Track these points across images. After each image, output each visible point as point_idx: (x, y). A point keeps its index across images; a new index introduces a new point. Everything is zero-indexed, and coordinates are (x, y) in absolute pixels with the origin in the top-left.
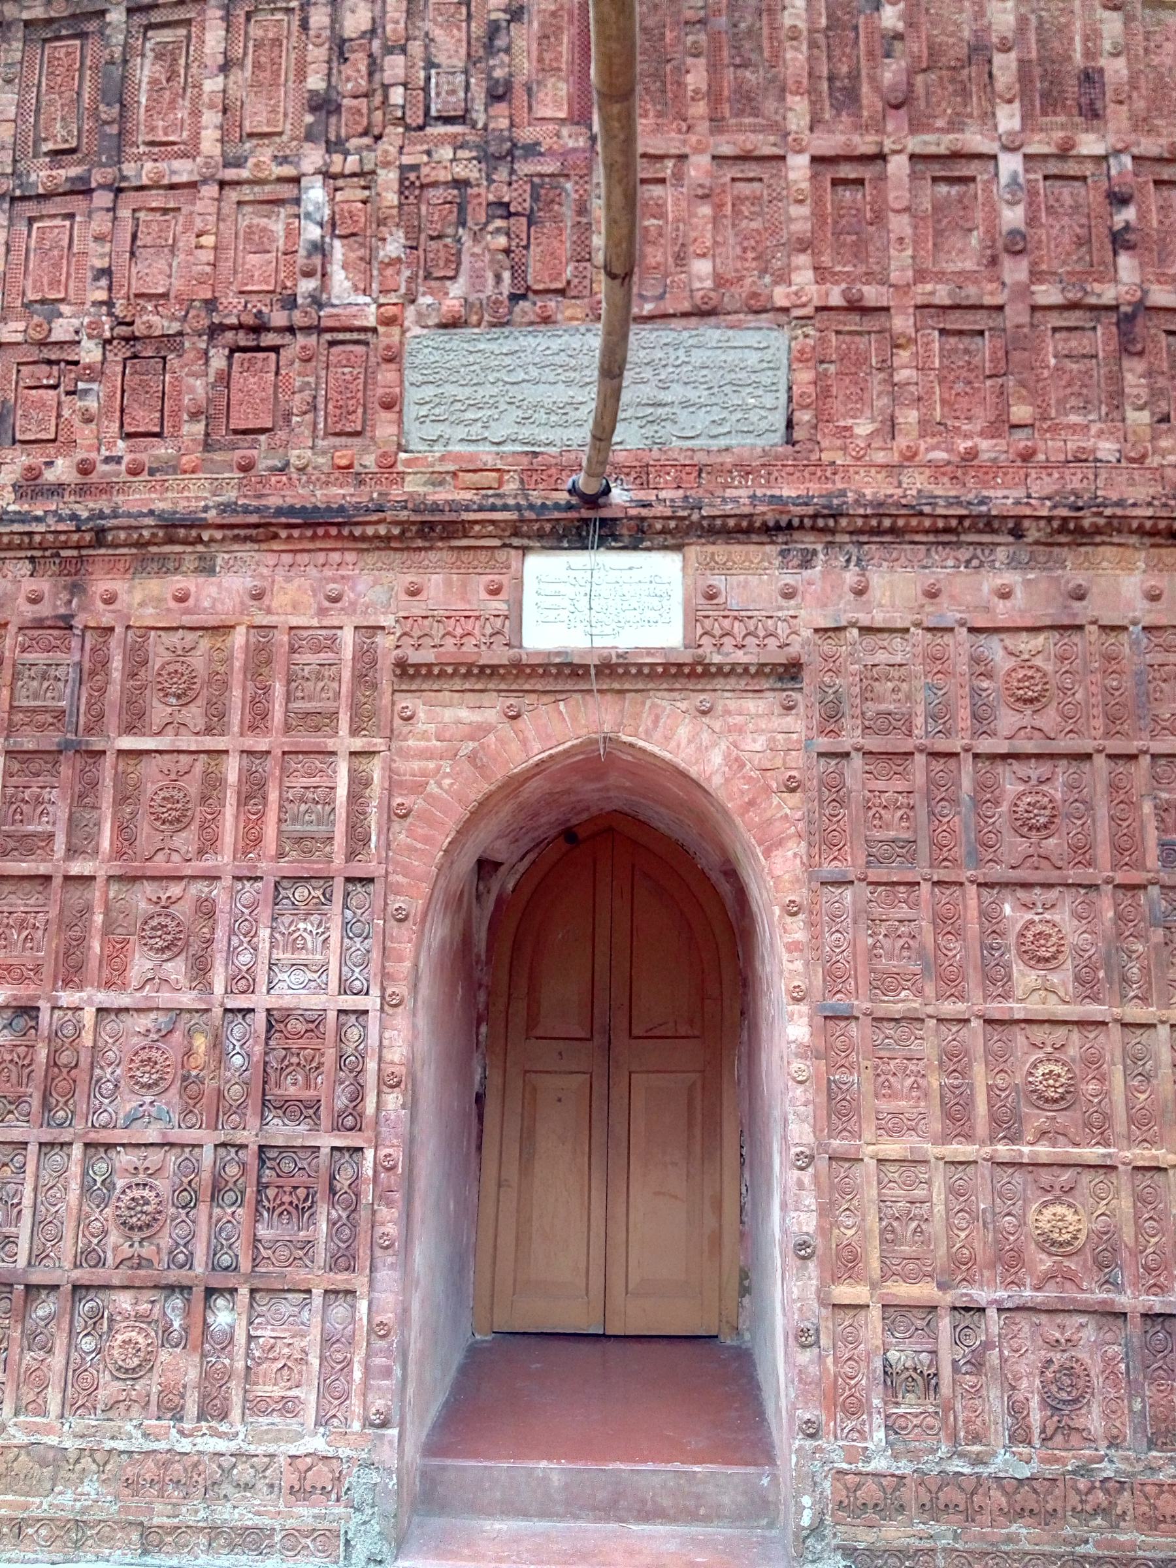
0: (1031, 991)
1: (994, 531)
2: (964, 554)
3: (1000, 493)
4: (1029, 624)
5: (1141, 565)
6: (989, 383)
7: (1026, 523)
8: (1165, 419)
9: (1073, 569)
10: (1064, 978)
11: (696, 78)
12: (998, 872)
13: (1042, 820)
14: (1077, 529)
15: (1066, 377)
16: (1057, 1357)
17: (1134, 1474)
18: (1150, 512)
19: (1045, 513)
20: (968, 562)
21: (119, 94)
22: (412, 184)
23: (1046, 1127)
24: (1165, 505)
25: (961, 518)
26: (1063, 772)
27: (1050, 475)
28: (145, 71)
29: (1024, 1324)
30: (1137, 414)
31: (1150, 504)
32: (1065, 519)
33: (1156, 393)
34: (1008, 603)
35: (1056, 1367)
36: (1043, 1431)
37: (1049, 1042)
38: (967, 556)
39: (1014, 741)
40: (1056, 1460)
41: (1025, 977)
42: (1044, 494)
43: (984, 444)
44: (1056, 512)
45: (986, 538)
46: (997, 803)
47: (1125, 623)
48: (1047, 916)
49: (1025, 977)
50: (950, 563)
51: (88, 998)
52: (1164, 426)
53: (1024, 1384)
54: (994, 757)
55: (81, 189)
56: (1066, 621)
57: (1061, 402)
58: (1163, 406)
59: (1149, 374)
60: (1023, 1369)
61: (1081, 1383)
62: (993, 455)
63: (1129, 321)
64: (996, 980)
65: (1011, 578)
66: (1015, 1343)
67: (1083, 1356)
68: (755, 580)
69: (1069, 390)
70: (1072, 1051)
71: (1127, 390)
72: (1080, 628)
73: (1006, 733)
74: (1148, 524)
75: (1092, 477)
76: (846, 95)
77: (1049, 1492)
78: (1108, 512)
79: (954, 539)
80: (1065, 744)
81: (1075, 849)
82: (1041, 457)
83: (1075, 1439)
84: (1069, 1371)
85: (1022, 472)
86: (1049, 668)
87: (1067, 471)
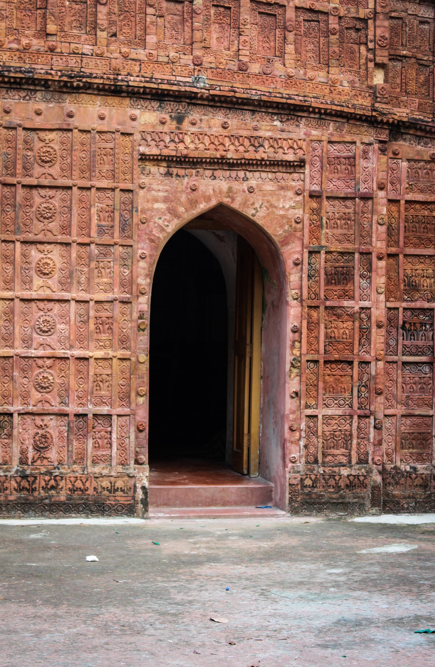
0: (39, 287)
1: (35, 85)
2: (23, 94)
3: (39, 67)
4: (49, 127)
5: (98, 103)
6: (39, 11)
7: (50, 83)
8: (115, 35)
9: (69, 104)
10: (53, 282)
12: (31, 237)
13: (49, 215)
14: (72, 86)
15: (73, 11)
16: (40, 432)
17: (67, 474)
18: (101, 81)
19: (57, 78)
20: (24, 97)
23: (42, 342)
24: (108, 78)
25: (21, 78)
26: (59, 194)
27: (62, 59)
29: (28, 419)
30: (102, 33)
31: (102, 78)
32: (66, 82)
33: (112, 23)
34: (40, 117)
35: (40, 435)
36: (33, 459)
37: (46, 308)
38: (24, 94)
39: (40, 179)
40: (37, 469)
41: (38, 281)
42: (59, 68)
43: (35, 42)
44: (62, 79)
45: (32, 87)
46: (31, 206)
47: (90, 129)
48: (49, 256)
50: (17, 97)
52: (114, 38)
53: (27, 442)
54: (31, 187)
56: (65, 127)
57: (71, 23)
58: (114, 29)
59: (109, 13)
60: (26, 436)
61: (49, 441)
62: (38, 48)
65: (42, 106)
66: (24, 427)
67: (51, 431)
69: (74, 18)
70: (55, 311)
71: (98, 21)
72: (71, 130)
73: (37, 176)
74: (101, 86)
75: (79, 61)
77: (34, 482)
78: (84, 80)
79: (18, 87)
80: (62, 182)
81: (62, 227)
82: (59, 50)
83: (45, 462)
84: (44, 436)
85: (50, 57)
86: (57, 147)
87: (69, 58)
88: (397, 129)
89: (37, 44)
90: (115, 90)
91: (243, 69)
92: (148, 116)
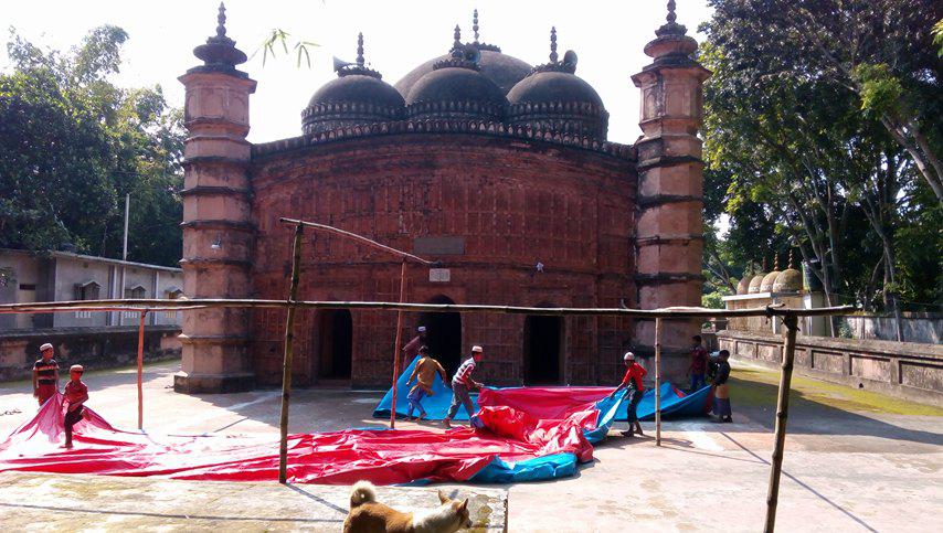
11: (453, 201)
21: (373, 200)
22: (414, 216)
28: (377, 198)
41: (491, 324)
49: (491, 324)
51: (375, 327)
55: (369, 215)
63: (507, 238)
64: (488, 325)
68: (460, 272)
76: (472, 202)
88: (600, 277)
89: (490, 256)
90: (513, 267)
91: (551, 259)
92: (522, 275)
